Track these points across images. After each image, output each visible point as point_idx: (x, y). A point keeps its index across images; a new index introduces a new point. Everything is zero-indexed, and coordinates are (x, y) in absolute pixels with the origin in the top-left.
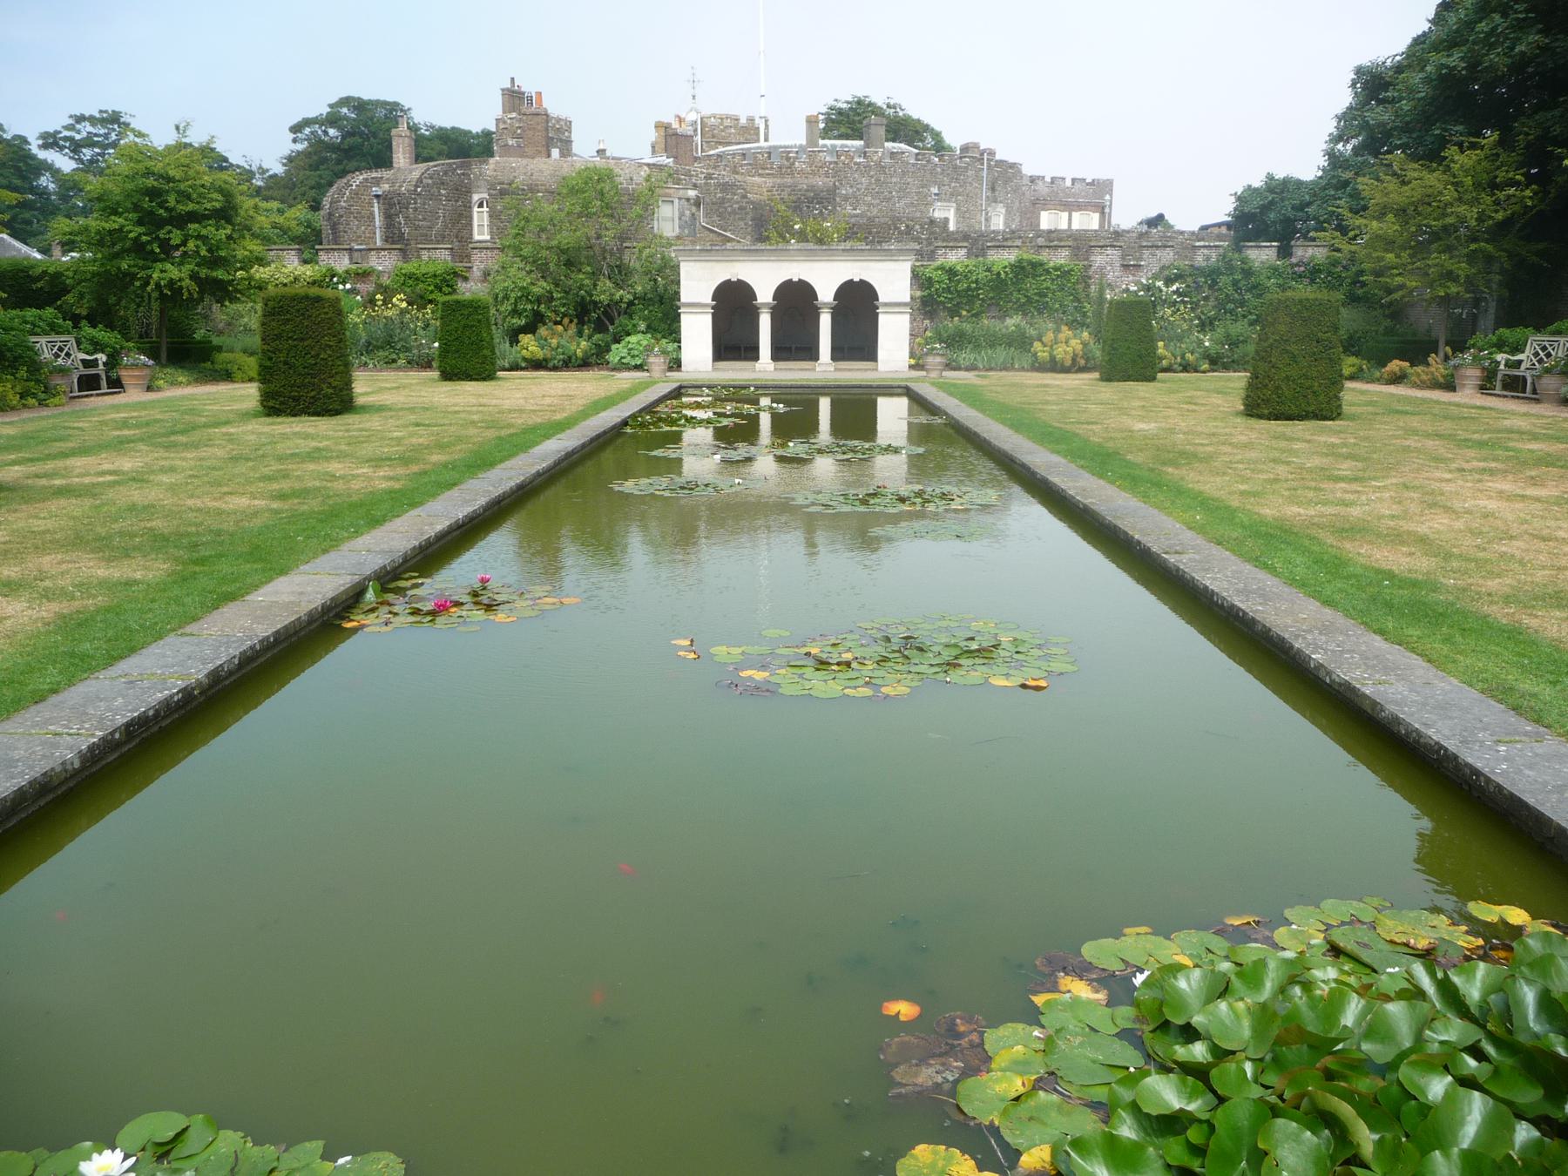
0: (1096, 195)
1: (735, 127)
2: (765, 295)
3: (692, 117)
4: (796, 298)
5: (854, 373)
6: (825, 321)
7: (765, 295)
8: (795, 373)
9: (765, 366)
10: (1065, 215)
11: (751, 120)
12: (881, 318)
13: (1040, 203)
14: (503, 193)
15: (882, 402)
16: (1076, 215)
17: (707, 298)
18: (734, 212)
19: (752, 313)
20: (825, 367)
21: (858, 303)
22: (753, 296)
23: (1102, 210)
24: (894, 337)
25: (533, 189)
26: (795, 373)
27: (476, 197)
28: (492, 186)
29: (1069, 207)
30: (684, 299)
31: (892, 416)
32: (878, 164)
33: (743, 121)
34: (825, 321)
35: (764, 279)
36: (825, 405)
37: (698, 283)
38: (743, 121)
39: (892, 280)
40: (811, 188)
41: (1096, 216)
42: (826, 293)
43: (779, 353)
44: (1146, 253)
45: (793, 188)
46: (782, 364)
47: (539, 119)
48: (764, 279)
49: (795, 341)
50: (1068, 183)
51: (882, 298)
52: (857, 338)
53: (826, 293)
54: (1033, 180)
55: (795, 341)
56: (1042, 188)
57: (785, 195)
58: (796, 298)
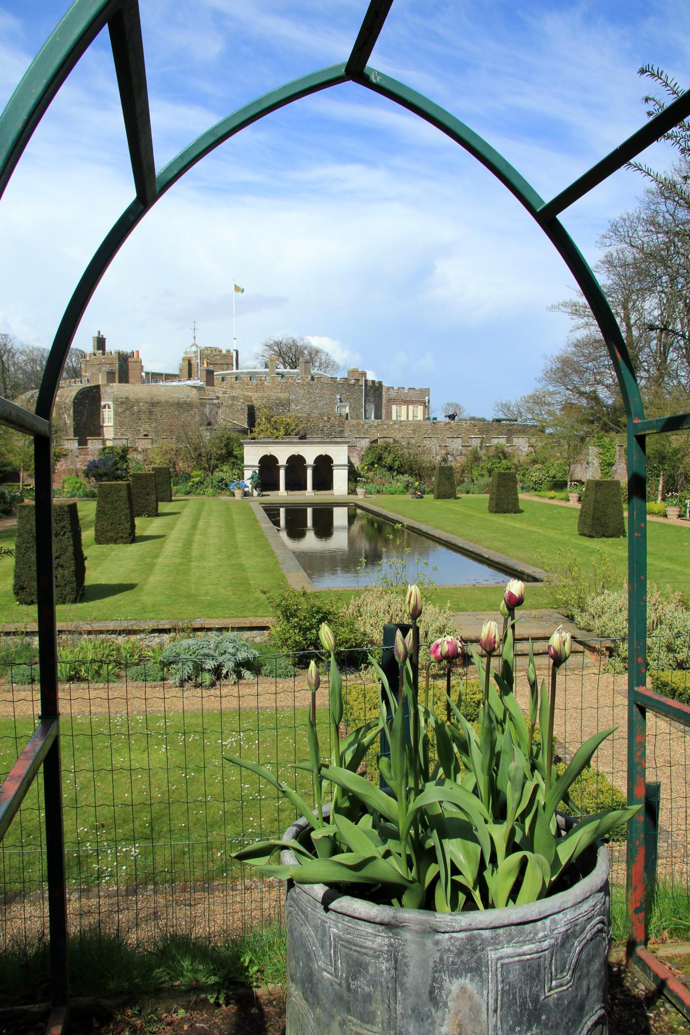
0: (420, 398)
1: (219, 355)
2: (282, 461)
3: (194, 349)
4: (296, 462)
5: (323, 496)
6: (309, 472)
7: (282, 461)
8: (297, 497)
9: (282, 494)
10: (404, 408)
11: (228, 351)
12: (335, 471)
13: (391, 401)
14: (122, 403)
15: (335, 509)
16: (411, 407)
17: (257, 464)
18: (238, 411)
19: (278, 468)
20: (309, 494)
21: (324, 465)
22: (277, 462)
23: (426, 406)
24: (340, 478)
25: (138, 401)
26: (297, 497)
27: (103, 403)
28: (115, 400)
29: (407, 402)
30: (246, 463)
31: (340, 516)
32: (308, 383)
33: (224, 352)
34: (309, 472)
35: (282, 454)
36: (310, 511)
37: (252, 455)
38: (224, 352)
39: (339, 455)
40: (278, 398)
41: (420, 409)
42: (310, 461)
43: (289, 487)
44: (450, 440)
45: (268, 398)
46: (291, 493)
47: (136, 364)
48: (282, 454)
49: (296, 483)
50: (406, 389)
51: (335, 463)
52: (324, 481)
53: (310, 461)
54: (388, 388)
55: (296, 483)
56: (393, 394)
57: (264, 402)
58: (296, 462)
